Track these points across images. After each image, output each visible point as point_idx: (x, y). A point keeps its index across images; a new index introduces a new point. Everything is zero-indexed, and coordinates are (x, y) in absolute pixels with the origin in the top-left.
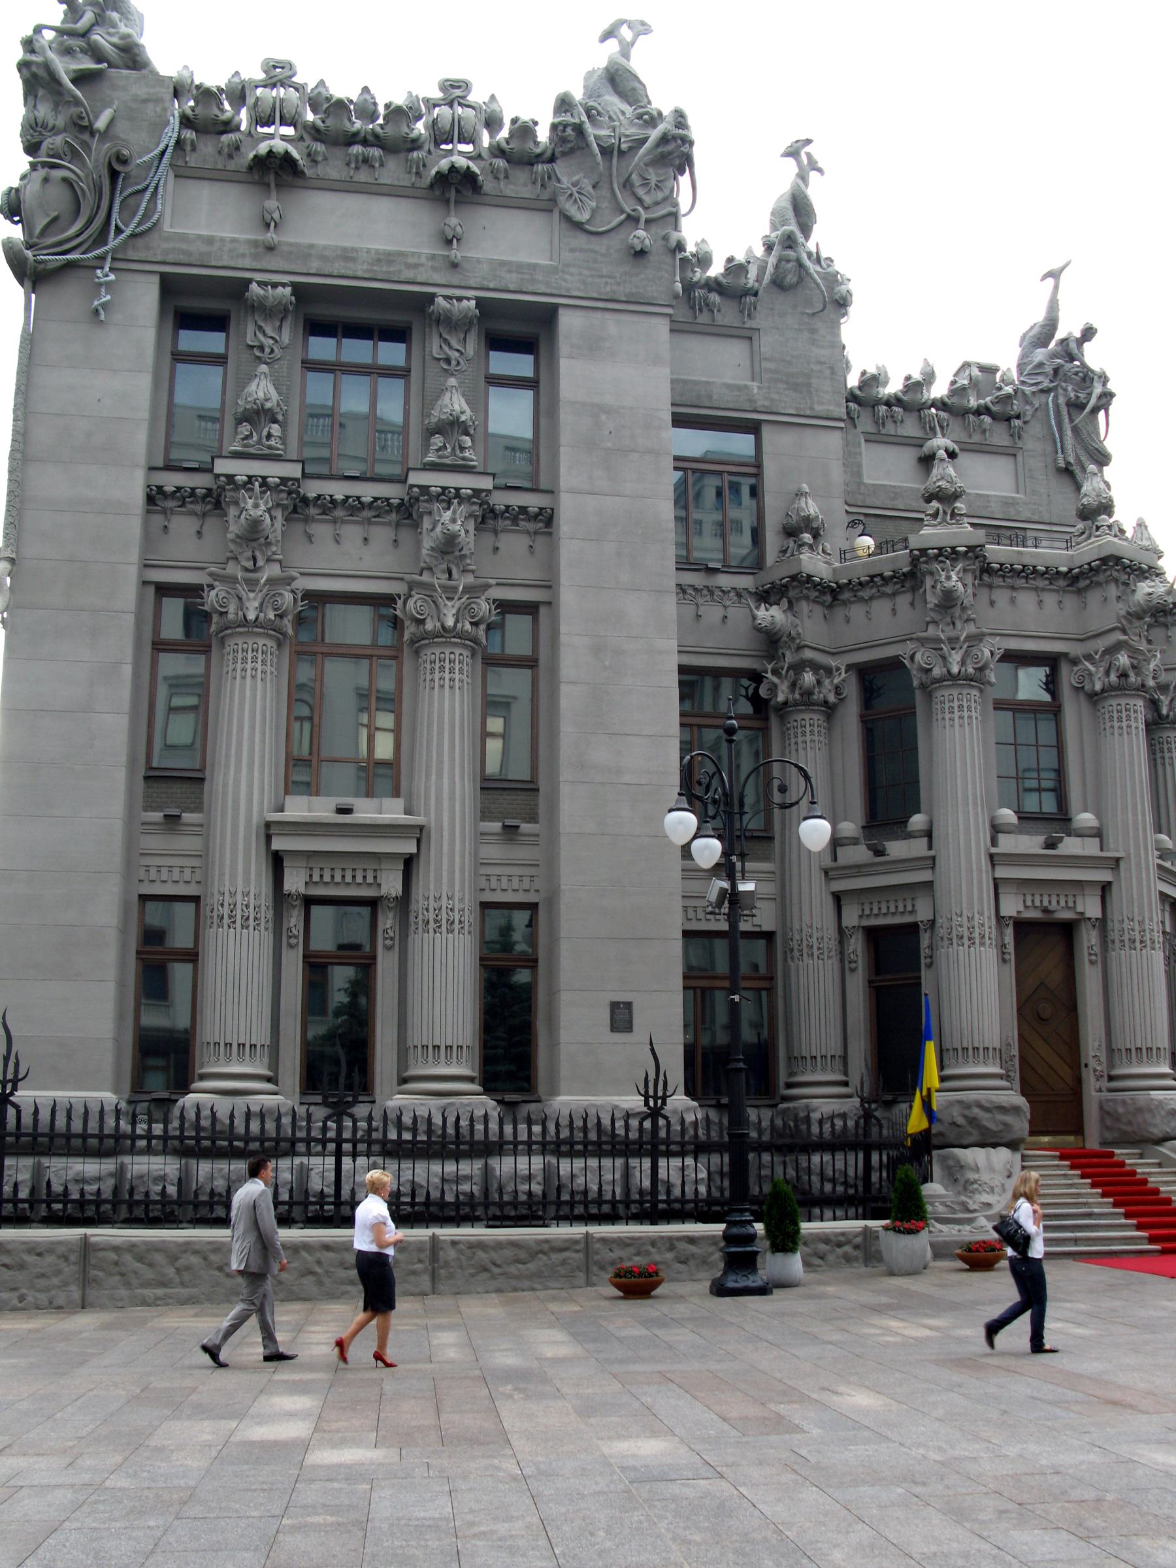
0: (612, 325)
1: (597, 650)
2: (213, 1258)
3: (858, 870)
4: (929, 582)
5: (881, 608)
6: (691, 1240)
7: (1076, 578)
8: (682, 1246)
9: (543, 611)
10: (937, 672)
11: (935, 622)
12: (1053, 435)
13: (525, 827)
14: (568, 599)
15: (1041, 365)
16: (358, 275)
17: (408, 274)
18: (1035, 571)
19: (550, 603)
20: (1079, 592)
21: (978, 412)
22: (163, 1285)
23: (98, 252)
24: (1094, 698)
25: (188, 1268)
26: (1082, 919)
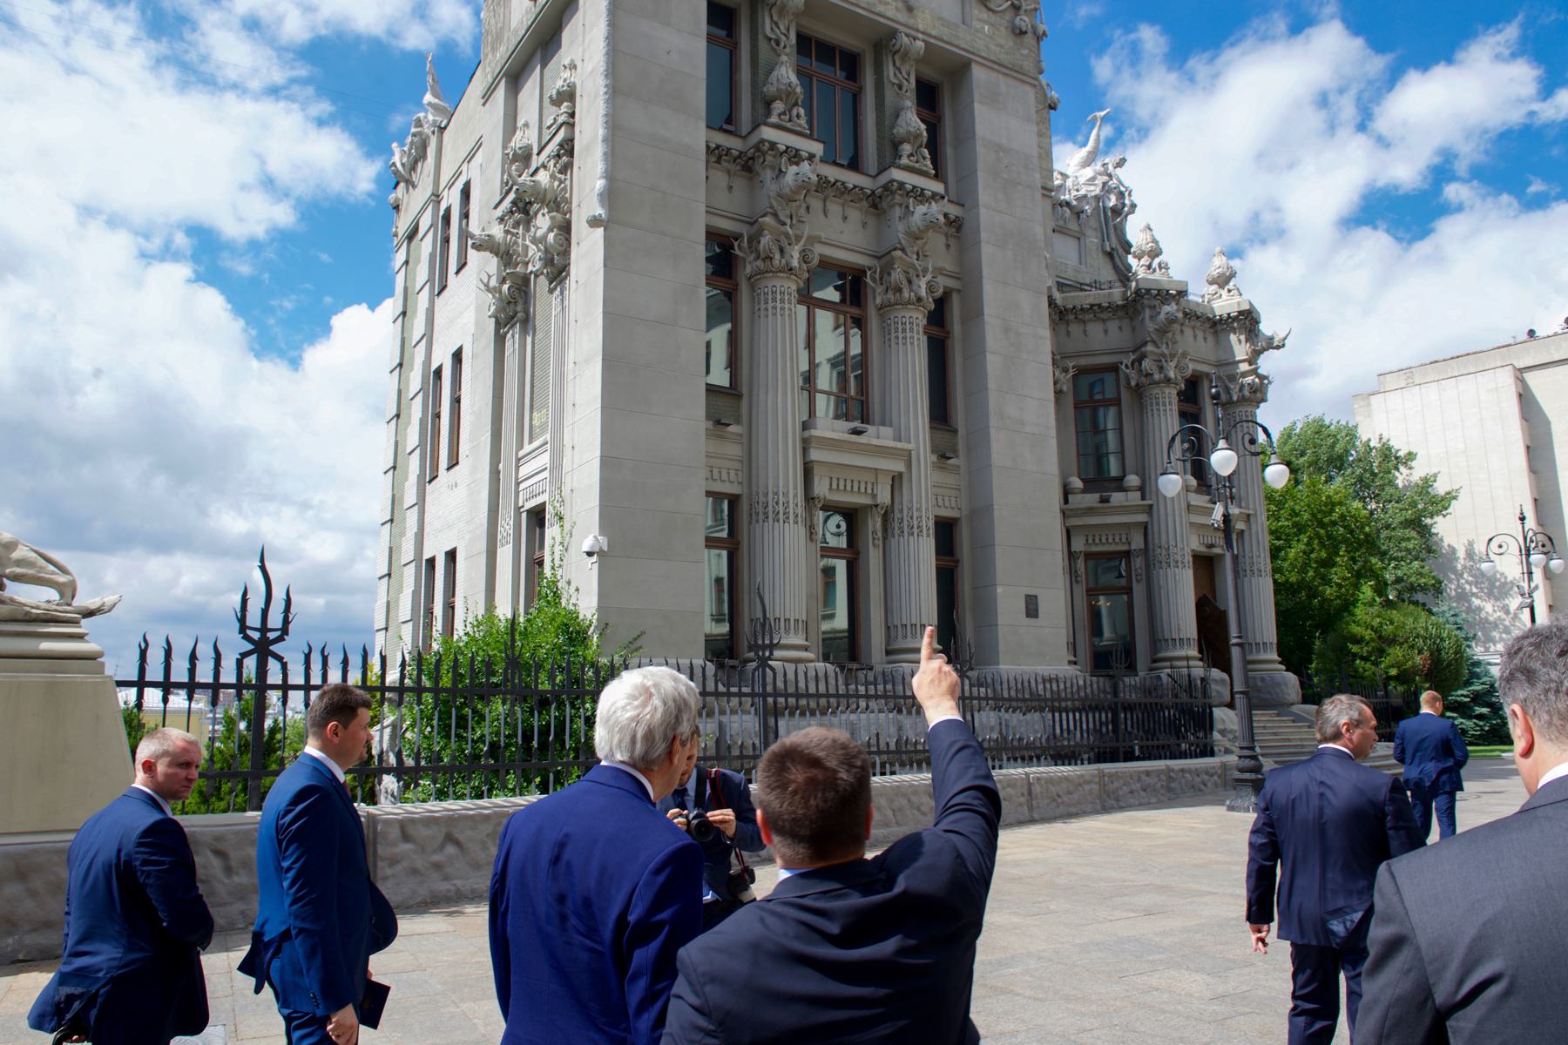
0: (1005, 85)
1: (1007, 330)
2: (914, 799)
3: (1090, 511)
4: (1148, 312)
5: (1095, 329)
6: (1148, 773)
8: (1144, 777)
9: (955, 297)
10: (1157, 377)
11: (1154, 342)
14: (989, 289)
15: (1093, 179)
17: (880, 8)
19: (959, 291)
20: (1216, 333)
22: (887, 825)
24: (1228, 405)
25: (901, 809)
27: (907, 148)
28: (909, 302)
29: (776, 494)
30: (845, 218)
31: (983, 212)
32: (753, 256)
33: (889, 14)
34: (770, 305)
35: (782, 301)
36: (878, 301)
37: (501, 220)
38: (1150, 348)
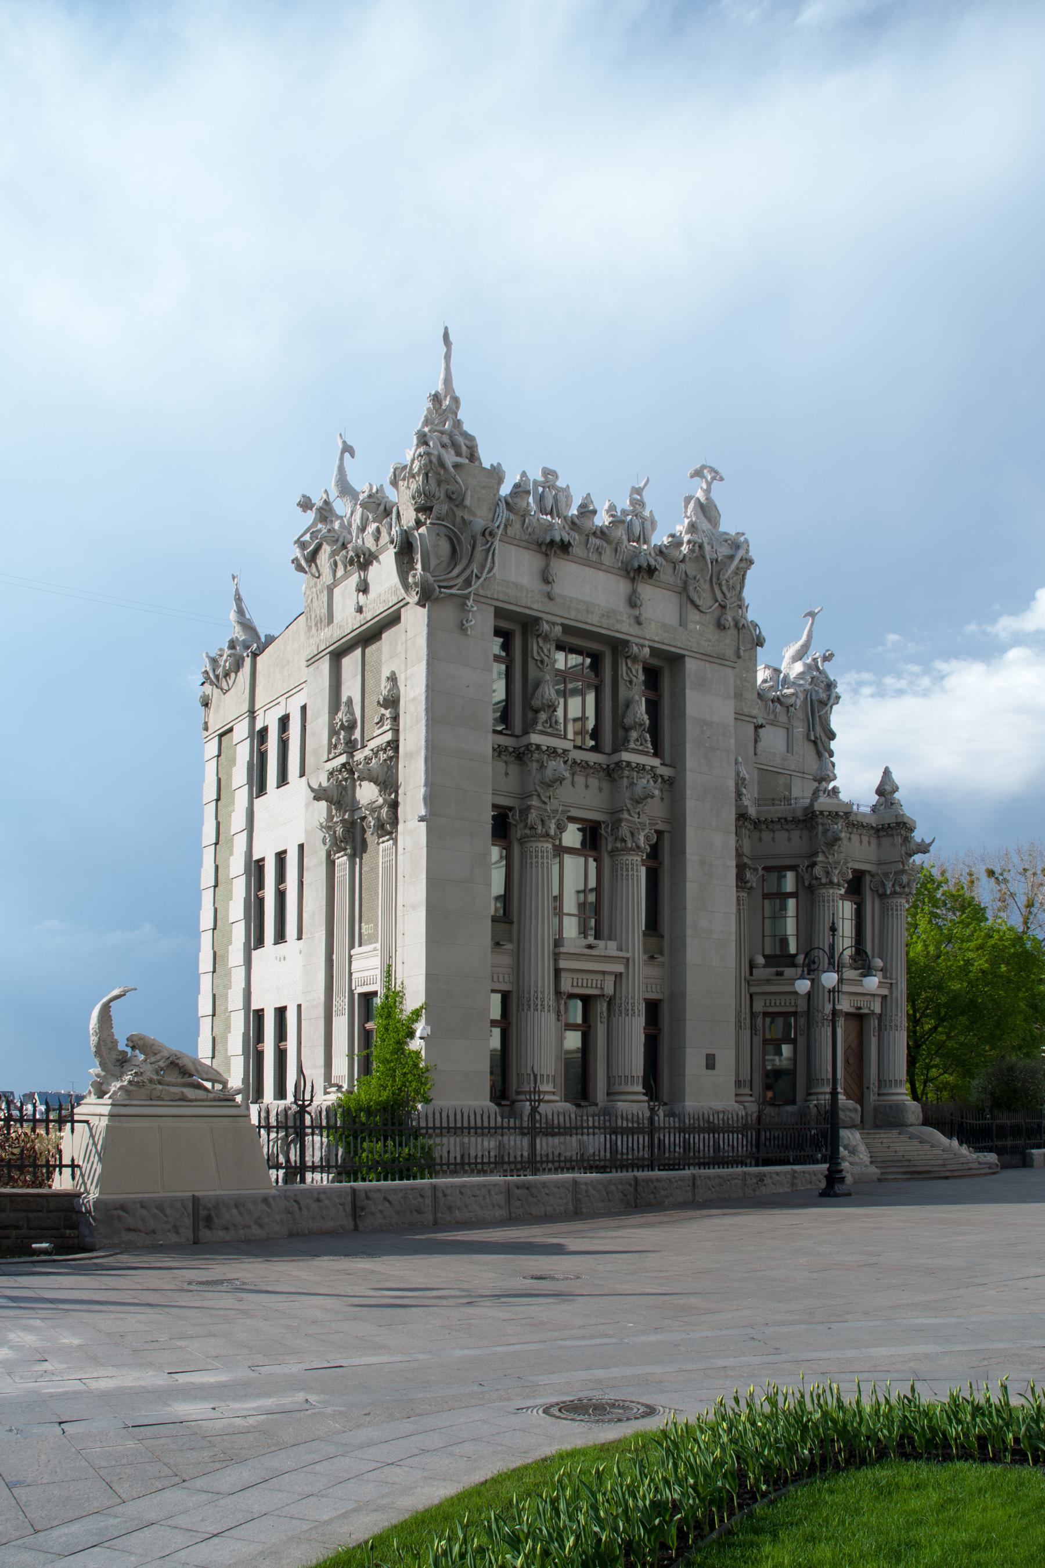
4: (820, 828)
5: (781, 836)
6: (777, 1174)
7: (878, 830)
8: (774, 1176)
11: (823, 852)
12: (808, 718)
13: (661, 959)
16: (593, 621)
17: (618, 627)
18: (862, 825)
20: (878, 837)
21: (773, 701)
23: (470, 590)
24: (883, 896)
26: (873, 1013)
27: (634, 735)
28: (632, 849)
29: (536, 992)
30: (587, 787)
31: (688, 774)
32: (522, 825)
33: (624, 630)
34: (534, 860)
35: (542, 857)
36: (609, 848)
37: (331, 773)
38: (820, 858)
